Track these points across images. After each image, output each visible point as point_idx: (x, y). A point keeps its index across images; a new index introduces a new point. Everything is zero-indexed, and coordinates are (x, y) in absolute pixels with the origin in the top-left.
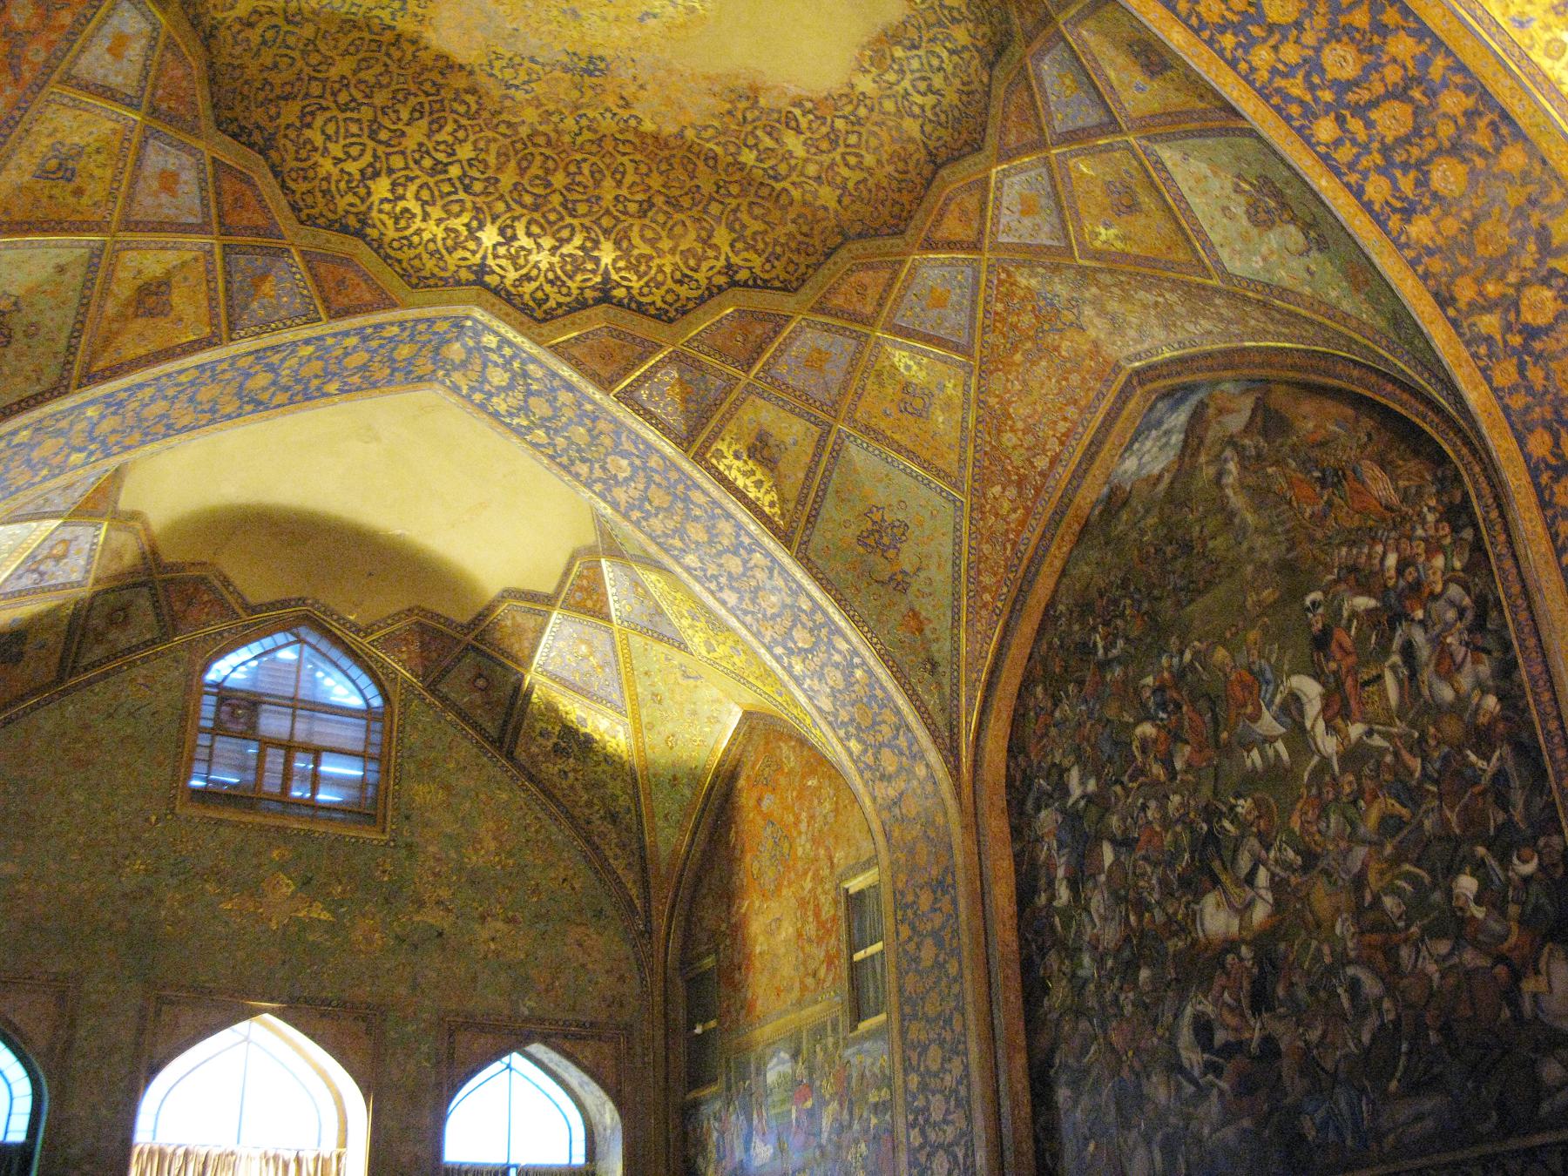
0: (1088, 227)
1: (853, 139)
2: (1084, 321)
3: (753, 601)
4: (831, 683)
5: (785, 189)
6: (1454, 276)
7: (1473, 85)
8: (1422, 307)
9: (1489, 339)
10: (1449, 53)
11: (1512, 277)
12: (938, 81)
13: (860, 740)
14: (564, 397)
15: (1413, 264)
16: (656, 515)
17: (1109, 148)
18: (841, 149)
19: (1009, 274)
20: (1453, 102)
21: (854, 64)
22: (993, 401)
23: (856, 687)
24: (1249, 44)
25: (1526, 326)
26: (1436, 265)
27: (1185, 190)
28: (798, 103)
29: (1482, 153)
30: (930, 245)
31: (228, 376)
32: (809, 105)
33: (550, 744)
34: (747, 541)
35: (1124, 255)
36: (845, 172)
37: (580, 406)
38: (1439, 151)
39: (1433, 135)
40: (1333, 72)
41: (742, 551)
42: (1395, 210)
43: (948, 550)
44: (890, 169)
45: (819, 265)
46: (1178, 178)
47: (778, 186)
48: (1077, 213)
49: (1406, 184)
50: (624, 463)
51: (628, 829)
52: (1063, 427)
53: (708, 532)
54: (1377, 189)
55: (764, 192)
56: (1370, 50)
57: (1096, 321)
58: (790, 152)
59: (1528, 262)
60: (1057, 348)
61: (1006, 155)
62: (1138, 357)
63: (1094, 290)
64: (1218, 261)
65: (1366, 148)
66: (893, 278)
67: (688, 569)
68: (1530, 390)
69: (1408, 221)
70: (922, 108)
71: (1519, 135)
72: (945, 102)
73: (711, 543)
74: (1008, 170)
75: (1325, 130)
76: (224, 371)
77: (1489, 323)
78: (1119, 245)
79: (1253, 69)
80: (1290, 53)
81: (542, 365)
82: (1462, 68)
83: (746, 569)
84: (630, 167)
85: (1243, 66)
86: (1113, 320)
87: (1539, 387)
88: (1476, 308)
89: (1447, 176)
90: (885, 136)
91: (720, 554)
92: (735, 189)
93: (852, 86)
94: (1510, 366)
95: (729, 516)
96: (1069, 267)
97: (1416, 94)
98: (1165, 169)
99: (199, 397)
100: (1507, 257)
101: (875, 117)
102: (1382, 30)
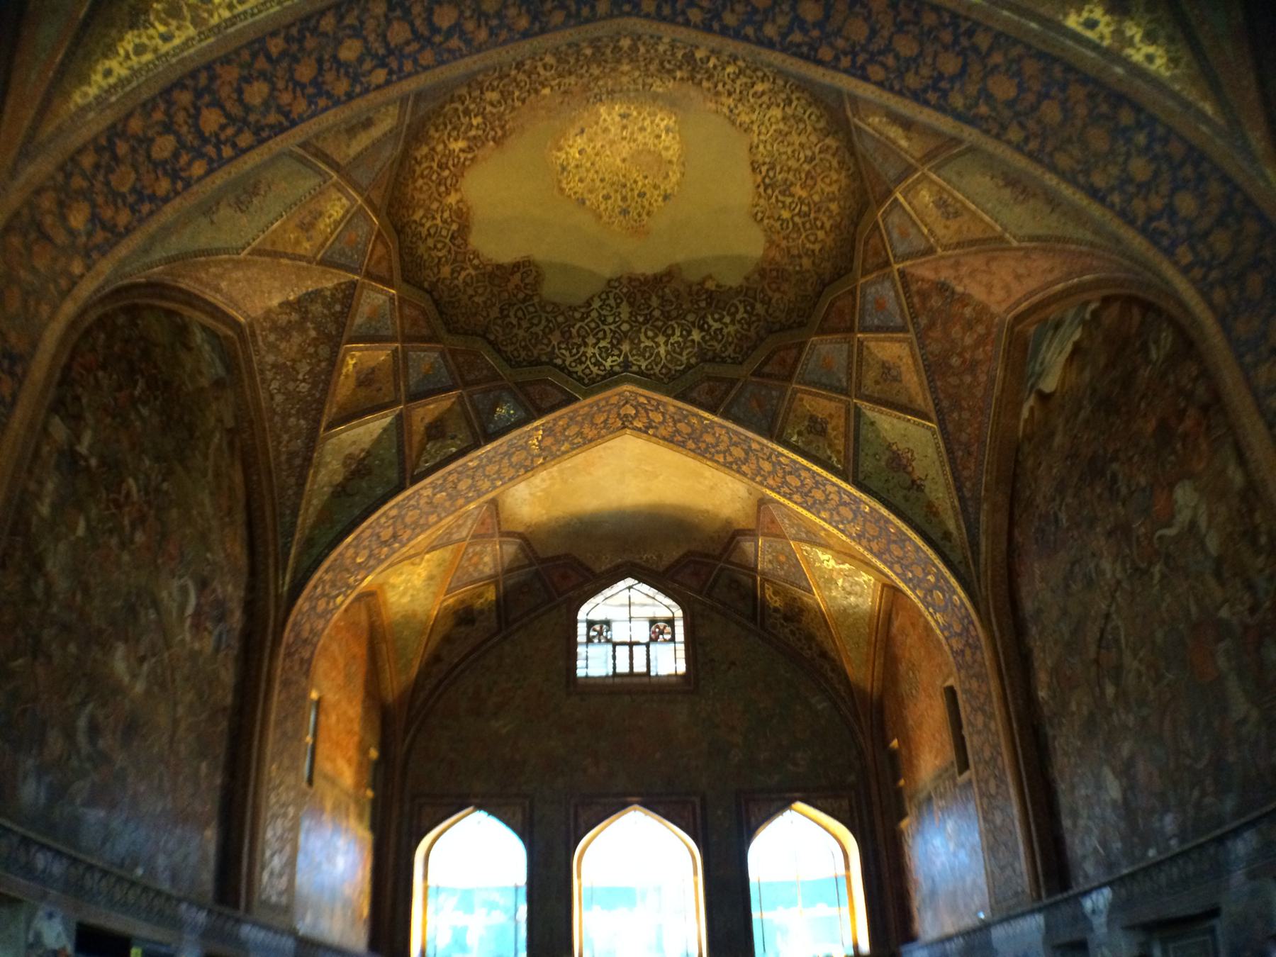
0: (358, 354)
1: (434, 177)
8: (326, 564)
12: (430, 242)
13: (97, 166)
14: (523, 23)
17: (397, 388)
24: (434, 488)
30: (379, 235)
31: (840, 43)
34: (322, 102)
35: (340, 374)
36: (424, 165)
37: (510, 29)
43: (217, 244)
49: (366, 543)
50: (445, 25)
62: (253, 334)
64: (332, 436)
66: (375, 211)
67: (322, 13)
72: (420, 243)
73: (335, 58)
75: (394, 512)
76: (846, 54)
77: (319, 589)
78: (344, 371)
80: (422, 502)
81: (556, 28)
84: (542, 72)
91: (320, 61)
93: (456, 190)
95: (350, 97)
99: (865, 31)
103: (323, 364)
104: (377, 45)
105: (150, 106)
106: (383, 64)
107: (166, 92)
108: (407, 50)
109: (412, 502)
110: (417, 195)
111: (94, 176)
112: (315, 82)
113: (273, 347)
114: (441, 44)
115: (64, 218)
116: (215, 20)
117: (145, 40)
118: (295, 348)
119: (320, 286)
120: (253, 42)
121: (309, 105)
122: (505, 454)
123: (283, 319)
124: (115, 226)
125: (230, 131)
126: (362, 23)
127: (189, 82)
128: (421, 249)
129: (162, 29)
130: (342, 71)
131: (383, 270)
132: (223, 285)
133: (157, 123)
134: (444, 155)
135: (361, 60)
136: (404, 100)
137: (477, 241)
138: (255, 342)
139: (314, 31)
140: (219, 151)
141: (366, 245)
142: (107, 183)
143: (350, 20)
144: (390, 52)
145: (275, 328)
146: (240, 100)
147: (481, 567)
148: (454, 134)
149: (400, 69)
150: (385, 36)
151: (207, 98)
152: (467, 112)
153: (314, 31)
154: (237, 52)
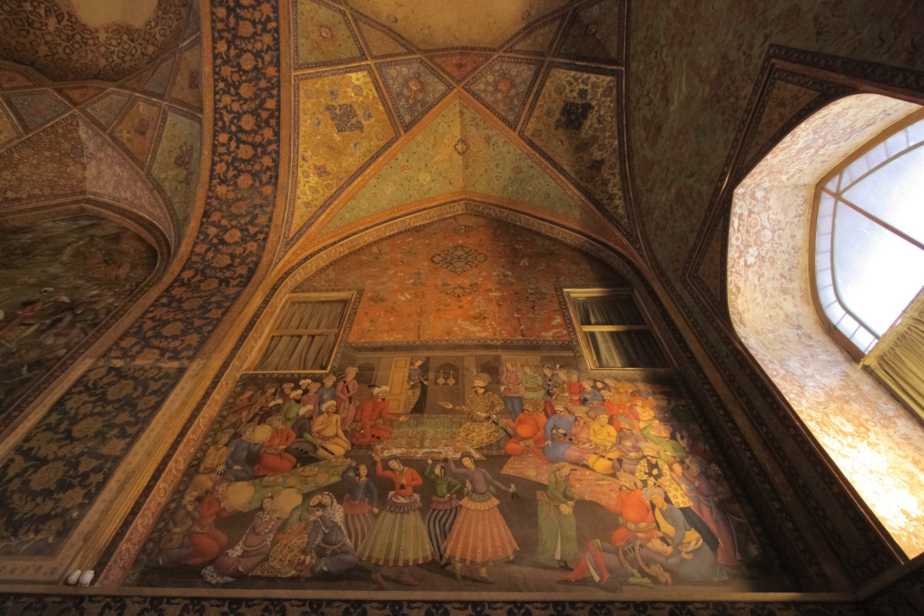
1: (77, 46)
2: (88, 167)
5: (28, 32)
6: (216, 210)
7: (276, 162)
9: (207, 235)
10: (278, 146)
11: (233, 223)
12: (128, 58)
15: (209, 197)
17: (154, 104)
19: (78, 125)
20: (267, 161)
22: (16, 155)
24: (226, 92)
25: (223, 239)
26: (215, 203)
27: (165, 134)
28: (70, 16)
29: (261, 182)
30: (60, 91)
32: (73, 20)
36: (60, 50)
38: (249, 172)
39: (253, 166)
40: (242, 123)
42: (219, 178)
44: (78, 65)
45: (7, 60)
46: (166, 129)
48: (123, 120)
49: (231, 173)
52: (36, 192)
54: (220, 168)
55: (19, 23)
56: (259, 127)
57: (93, 169)
58: (47, 24)
59: (243, 222)
60: (68, 166)
63: (102, 154)
64: (151, 167)
65: (229, 154)
68: (203, 258)
69: (220, 184)
70: (113, 61)
71: (275, 185)
72: (123, 65)
75: (223, 138)
77: (212, 231)
79: (220, 101)
80: (236, 107)
82: (278, 153)
85: (218, 97)
86: (99, 173)
87: (207, 259)
88: (213, 224)
89: (245, 181)
90: (90, 55)
93: (97, 31)
94: (205, 247)
96: (101, 136)
97: (259, 150)
98: (164, 123)
100: (238, 216)
101: (94, 48)
102: (267, 123)
109: (227, 118)
122: (230, 10)
134: (59, 36)
137: (138, 23)
138: (99, 195)
147: (518, 81)
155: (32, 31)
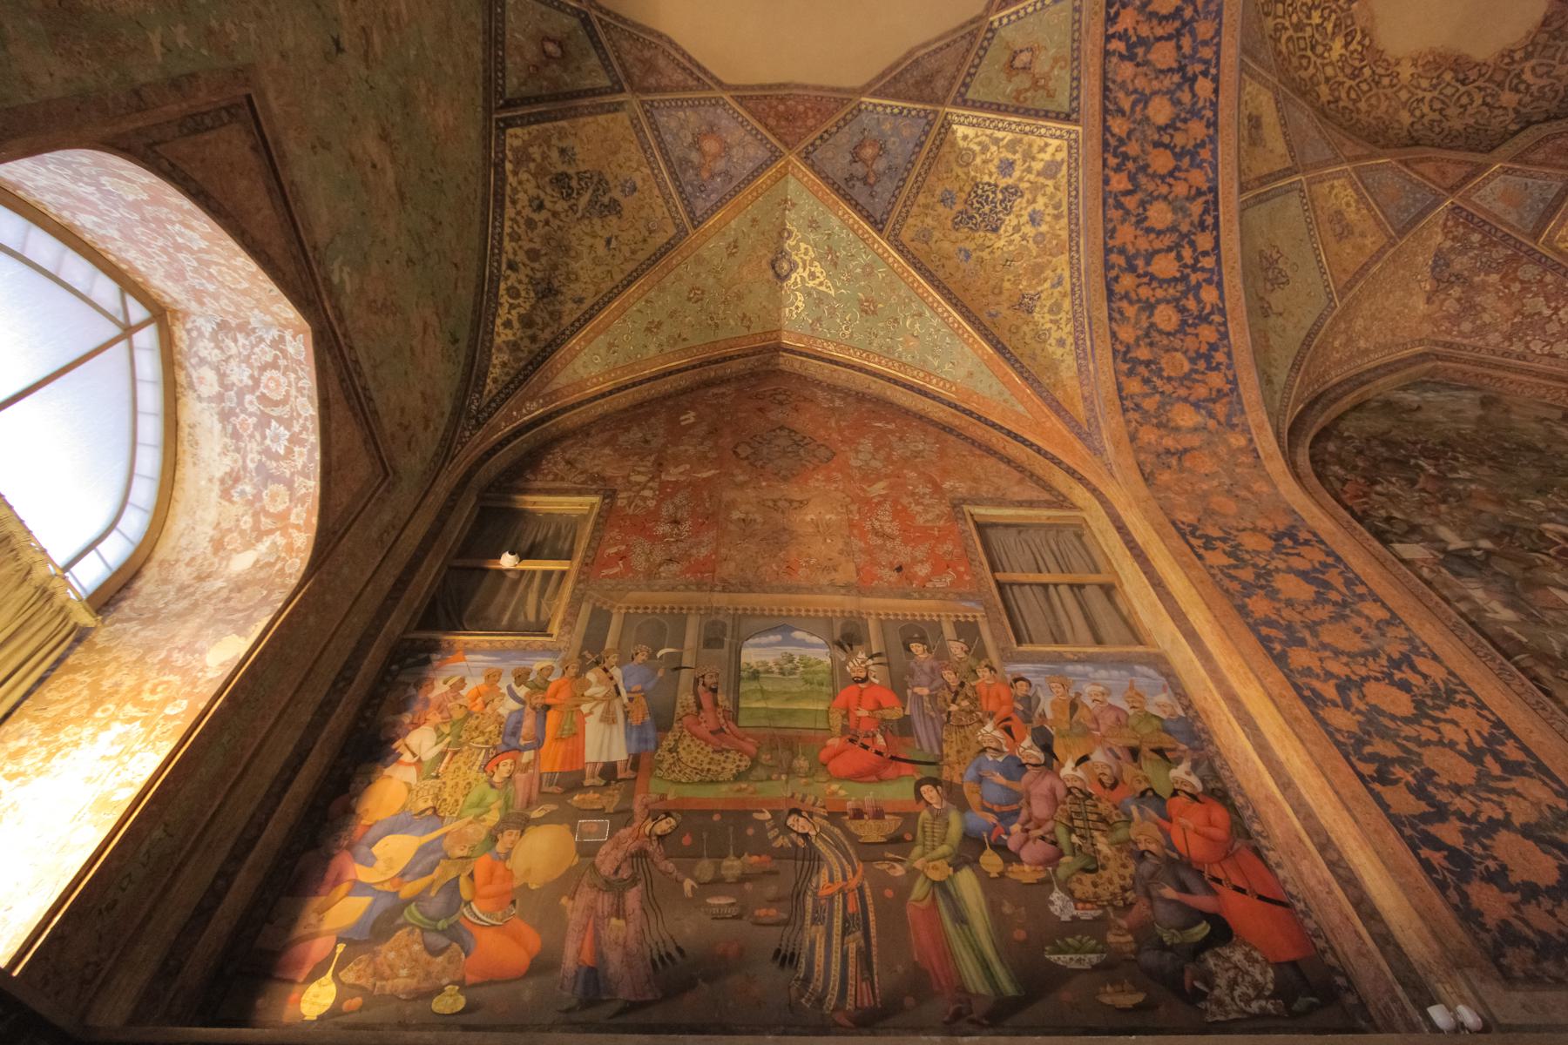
1: (1365, 87)
3: (1143, 204)
4: (1157, 319)
12: (1452, 111)
13: (1146, 381)
16: (1138, 65)
18: (1353, 83)
21: (1415, 55)
23: (1189, 339)
30: (1406, 164)
33: (561, 168)
34: (1205, 154)
36: (1343, 95)
41: (1187, 160)
43: (1308, 323)
47: (1309, 53)
51: (556, 316)
53: (1173, 121)
61: (1520, 158)
62: (1451, 345)
66: (1369, 157)
67: (1106, 129)
70: (1423, 116)
73: (1160, 129)
74: (1515, 171)
83: (1171, 174)
90: (1384, 105)
91: (1157, 144)
92: (1295, 19)
93: (1398, 63)
95: (1213, 124)
103: (1549, 278)
104: (1167, 82)
105: (1117, 316)
106: (1194, 79)
107: (1110, 294)
108: (1187, 50)
110: (1379, 113)
111: (1155, 388)
112: (1178, 156)
113: (1480, 331)
114: (1196, 10)
115: (1177, 429)
116: (1064, 234)
117: (1048, 303)
118: (1500, 305)
119: (1433, 250)
120: (1105, 203)
121: (1199, 166)
123: (1451, 306)
124: (1219, 391)
125: (1187, 253)
126: (1135, 91)
127: (1113, 273)
128: (1458, 125)
129: (1047, 285)
130: (1179, 124)
131: (1454, 173)
132: (1362, 344)
133: (1138, 315)
134: (1342, 69)
135: (1177, 103)
136: (1243, 68)
137: (1483, 49)
138: (1459, 347)
139: (1121, 142)
140: (1203, 269)
141: (1411, 181)
142: (1170, 379)
143: (1126, 105)
144: (1182, 69)
145: (1455, 319)
146: (1159, 233)
148: (1320, 49)
149: (1206, 62)
150: (1162, 71)
151: (1140, 263)
152: (1299, 27)
153: (1121, 142)
154: (1106, 220)
155: (1313, 58)
